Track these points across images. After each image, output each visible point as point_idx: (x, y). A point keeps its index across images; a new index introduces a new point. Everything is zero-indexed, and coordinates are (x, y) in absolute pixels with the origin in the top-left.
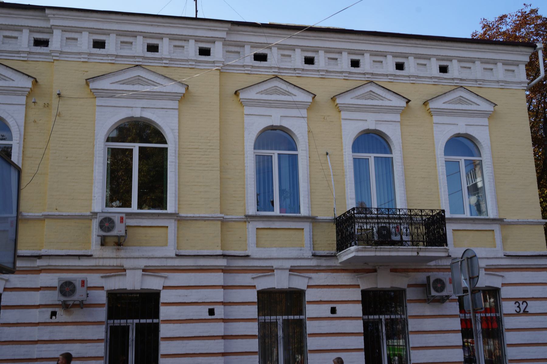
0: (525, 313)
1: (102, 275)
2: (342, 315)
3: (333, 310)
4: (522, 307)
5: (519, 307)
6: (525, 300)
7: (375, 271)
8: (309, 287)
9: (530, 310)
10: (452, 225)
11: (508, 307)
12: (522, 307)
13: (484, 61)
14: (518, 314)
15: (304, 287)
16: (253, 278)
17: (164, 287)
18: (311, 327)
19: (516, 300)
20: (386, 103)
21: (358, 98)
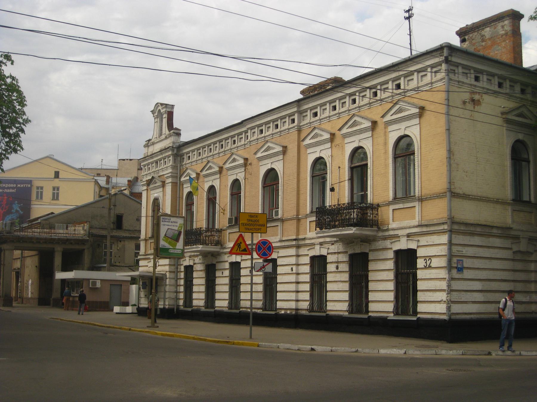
0: (430, 267)
1: (308, 248)
2: (341, 270)
3: (337, 268)
4: (428, 263)
5: (426, 262)
6: (430, 257)
7: (353, 242)
8: (328, 254)
9: (433, 265)
10: (392, 206)
11: (420, 263)
12: (428, 263)
13: (418, 71)
14: (425, 268)
15: (326, 255)
16: (308, 250)
17: (278, 257)
18: (330, 277)
19: (425, 258)
20: (363, 126)
21: (350, 127)
